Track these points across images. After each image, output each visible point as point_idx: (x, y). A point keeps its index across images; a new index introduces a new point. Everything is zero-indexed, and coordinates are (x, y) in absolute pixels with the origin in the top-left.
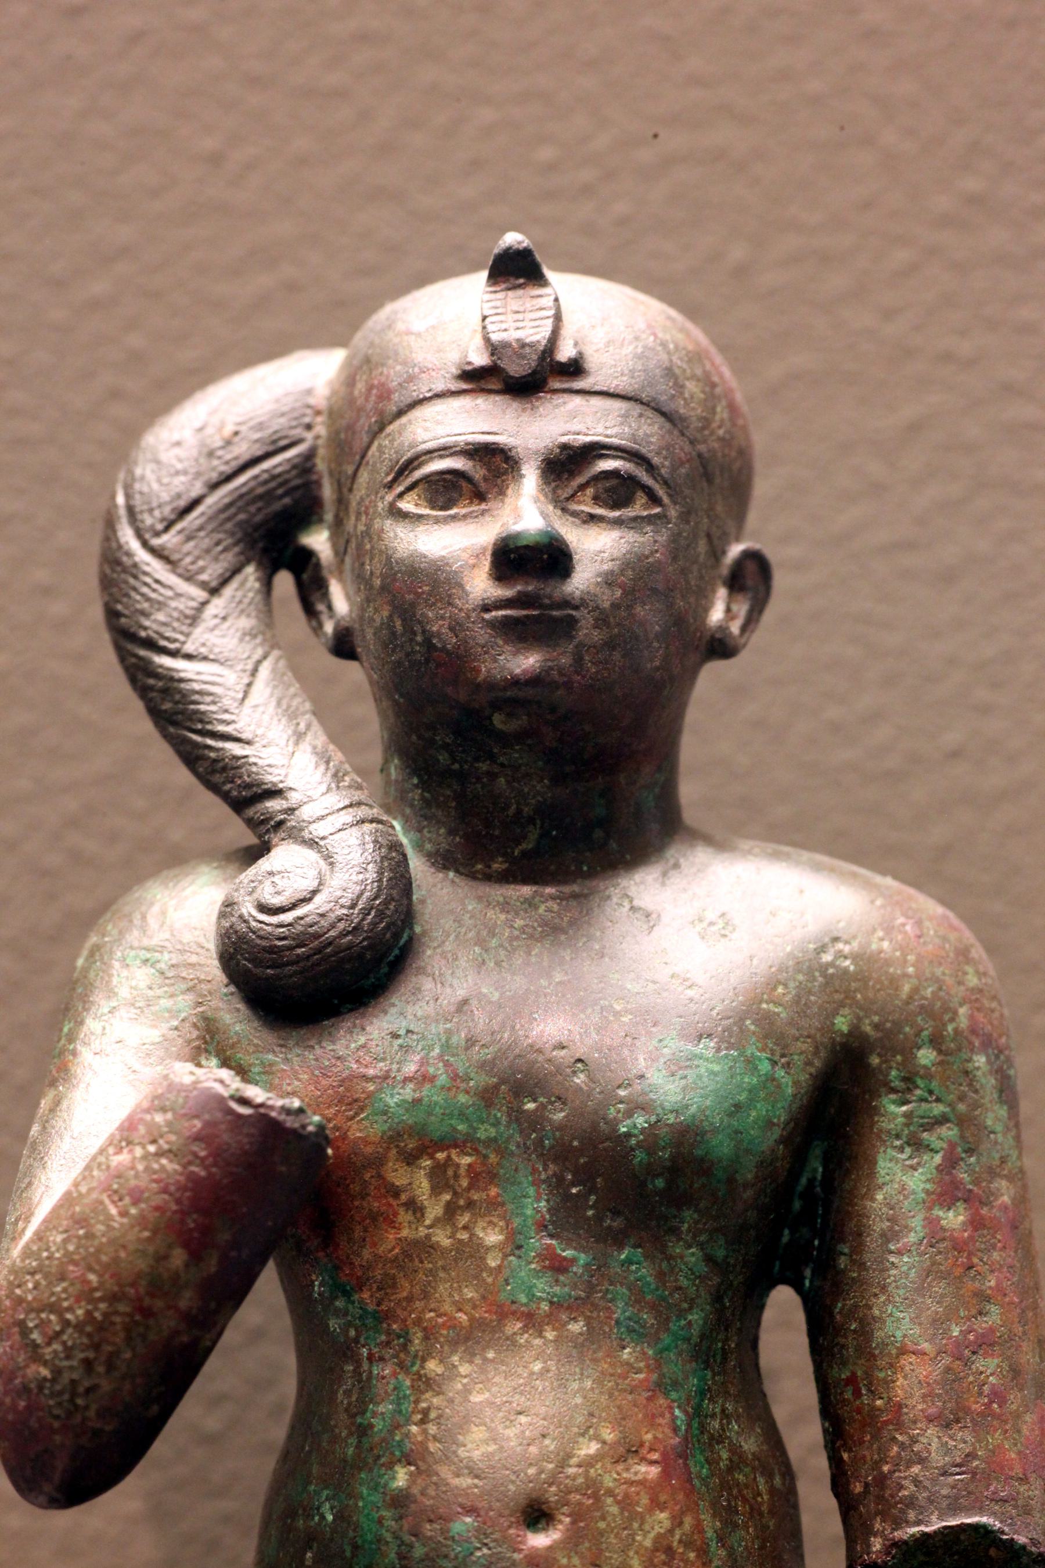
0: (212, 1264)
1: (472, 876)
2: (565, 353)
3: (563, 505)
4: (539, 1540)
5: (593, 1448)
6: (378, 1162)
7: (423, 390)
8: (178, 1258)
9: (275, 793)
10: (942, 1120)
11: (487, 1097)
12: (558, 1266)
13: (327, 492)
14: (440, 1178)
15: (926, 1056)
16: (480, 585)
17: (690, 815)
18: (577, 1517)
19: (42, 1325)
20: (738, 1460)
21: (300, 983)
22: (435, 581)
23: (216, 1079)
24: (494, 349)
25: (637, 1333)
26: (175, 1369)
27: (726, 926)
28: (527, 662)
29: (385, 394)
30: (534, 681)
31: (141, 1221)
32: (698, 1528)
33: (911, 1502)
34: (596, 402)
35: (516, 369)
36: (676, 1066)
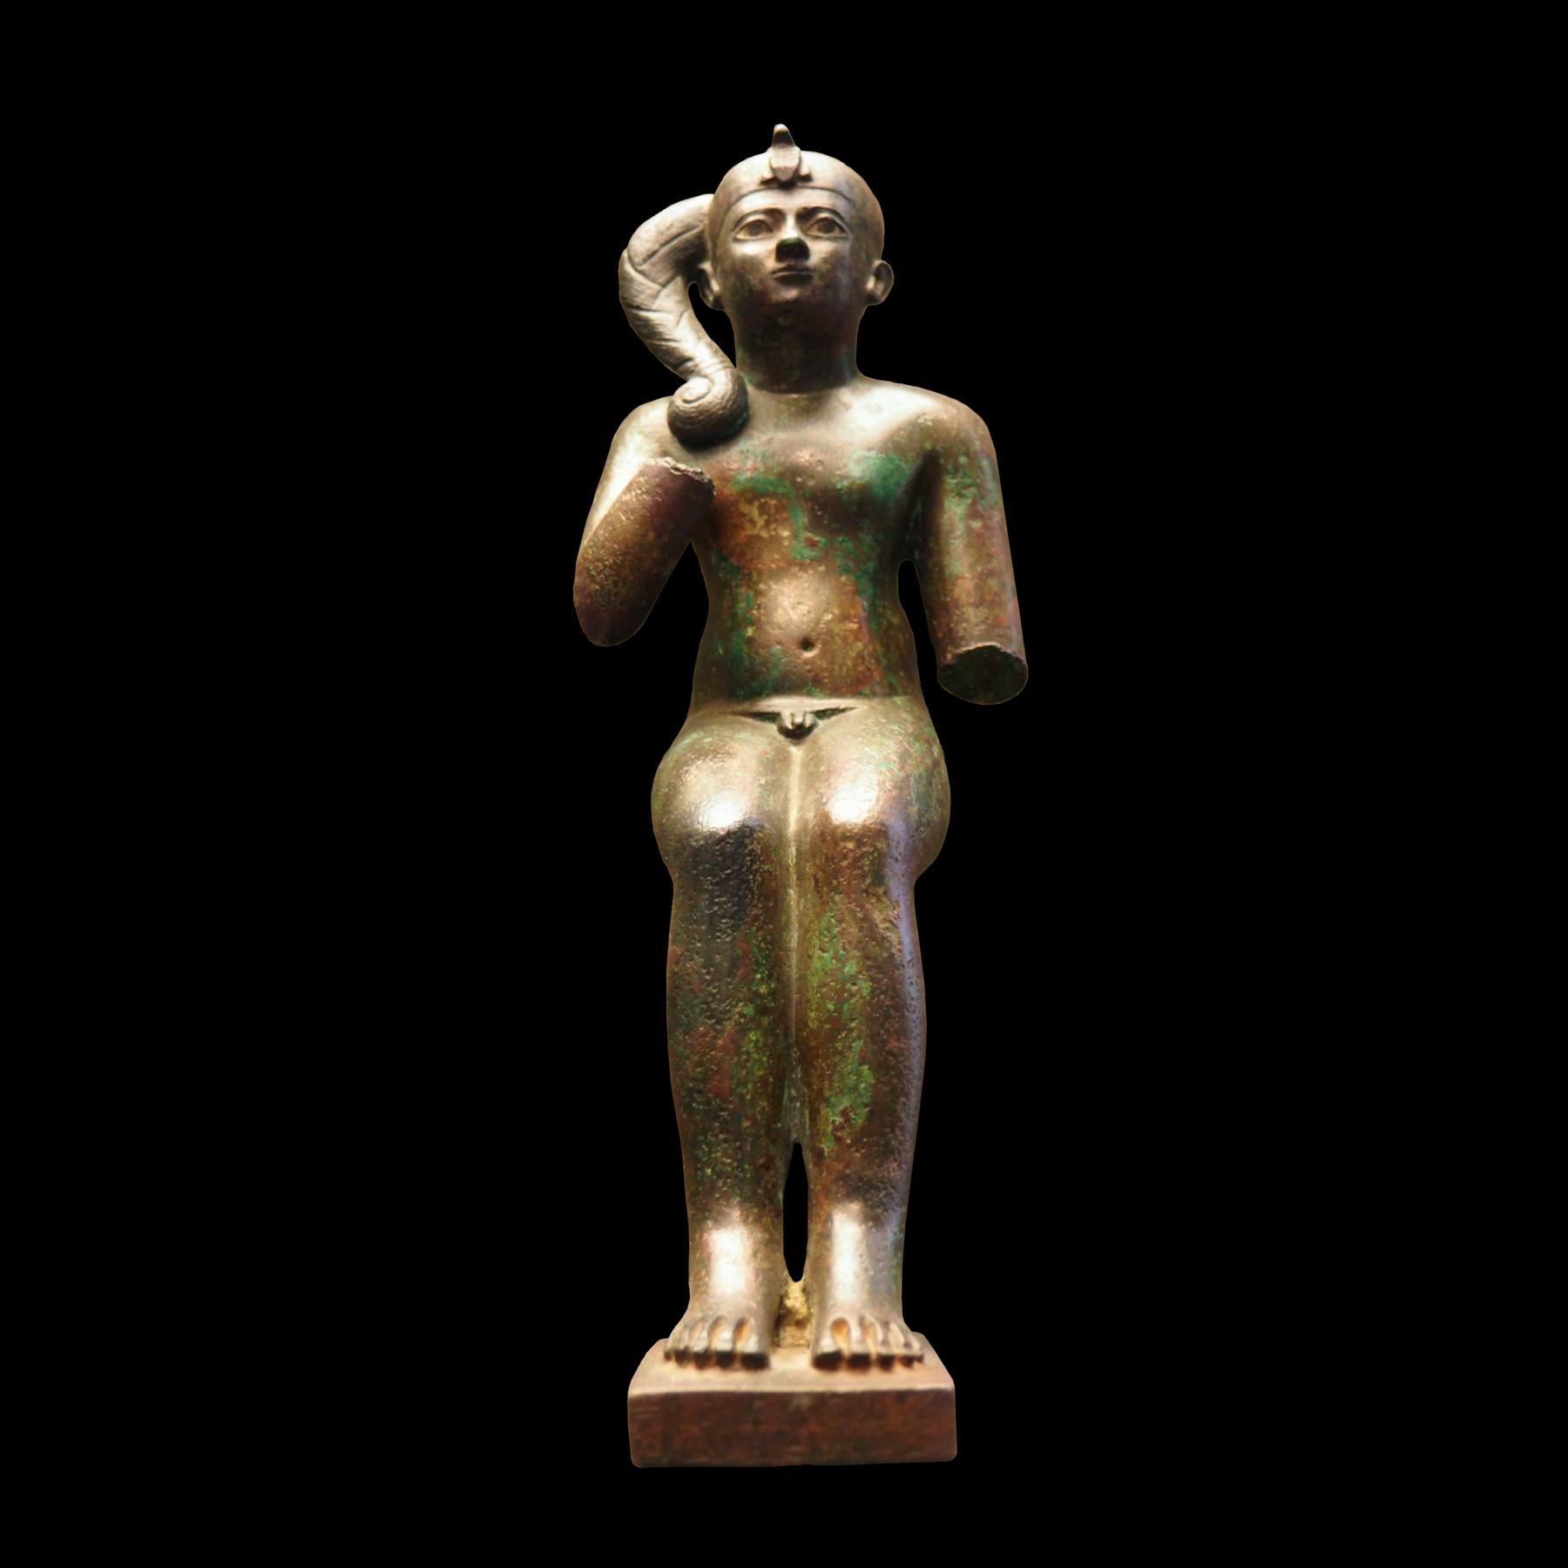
0: (666, 539)
1: (773, 391)
3: (804, 231)
4: (808, 655)
5: (829, 617)
6: (736, 503)
7: (745, 190)
8: (651, 535)
9: (690, 359)
10: (970, 486)
11: (781, 476)
12: (813, 544)
13: (709, 245)
14: (763, 509)
15: (963, 460)
16: (771, 264)
18: (824, 644)
19: (596, 568)
20: (890, 626)
21: (703, 433)
22: (751, 264)
23: (667, 462)
24: (773, 170)
25: (847, 571)
27: (879, 409)
28: (791, 294)
29: (730, 194)
30: (795, 301)
31: (635, 522)
32: (875, 650)
33: (962, 638)
34: (818, 192)
35: (783, 177)
36: (858, 461)
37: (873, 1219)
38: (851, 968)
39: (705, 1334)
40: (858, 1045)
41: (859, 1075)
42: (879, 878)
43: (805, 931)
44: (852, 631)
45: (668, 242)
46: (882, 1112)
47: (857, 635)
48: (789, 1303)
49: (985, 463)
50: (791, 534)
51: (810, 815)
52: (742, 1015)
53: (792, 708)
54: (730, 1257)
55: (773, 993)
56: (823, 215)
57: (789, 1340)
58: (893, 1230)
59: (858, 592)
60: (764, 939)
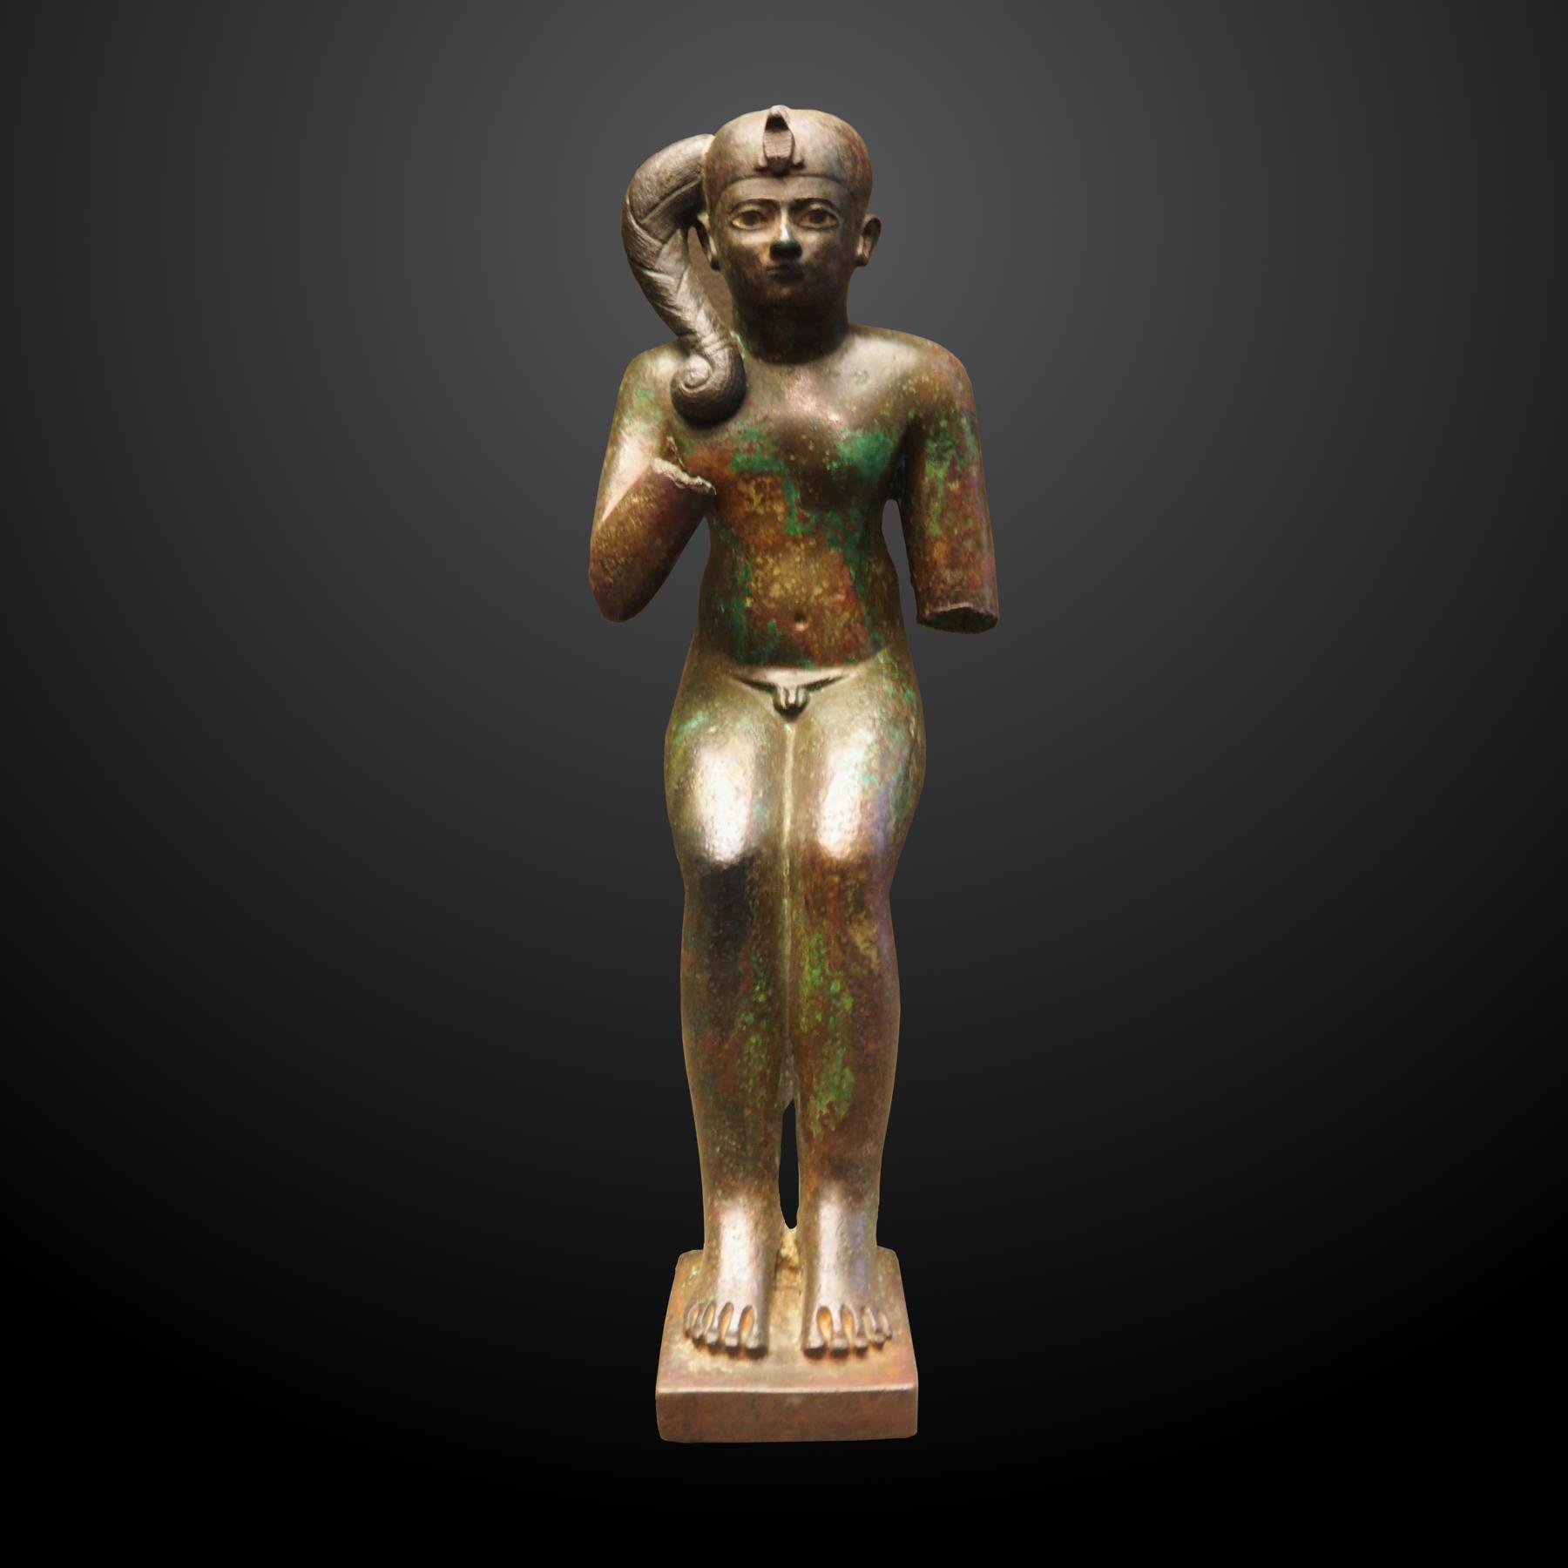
2: (797, 159)
4: (801, 627)
6: (735, 483)
8: (659, 542)
12: (804, 520)
14: (759, 488)
16: (765, 259)
17: (851, 320)
20: (875, 578)
21: (701, 414)
22: (749, 256)
25: (834, 543)
26: (659, 576)
28: (786, 291)
35: (778, 168)
37: (853, 1198)
38: (835, 987)
39: (714, 376)
40: (840, 1053)
41: (842, 1077)
42: (860, 905)
43: (796, 944)
44: (840, 602)
45: (668, 195)
46: (860, 1105)
47: (844, 605)
48: (784, 1252)
49: (964, 421)
50: (784, 510)
51: (802, 837)
52: (743, 1023)
53: (786, 680)
54: (736, 1231)
55: (770, 1000)
56: (816, 206)
57: (784, 1282)
58: (873, 1198)
59: (846, 562)
60: (762, 955)
